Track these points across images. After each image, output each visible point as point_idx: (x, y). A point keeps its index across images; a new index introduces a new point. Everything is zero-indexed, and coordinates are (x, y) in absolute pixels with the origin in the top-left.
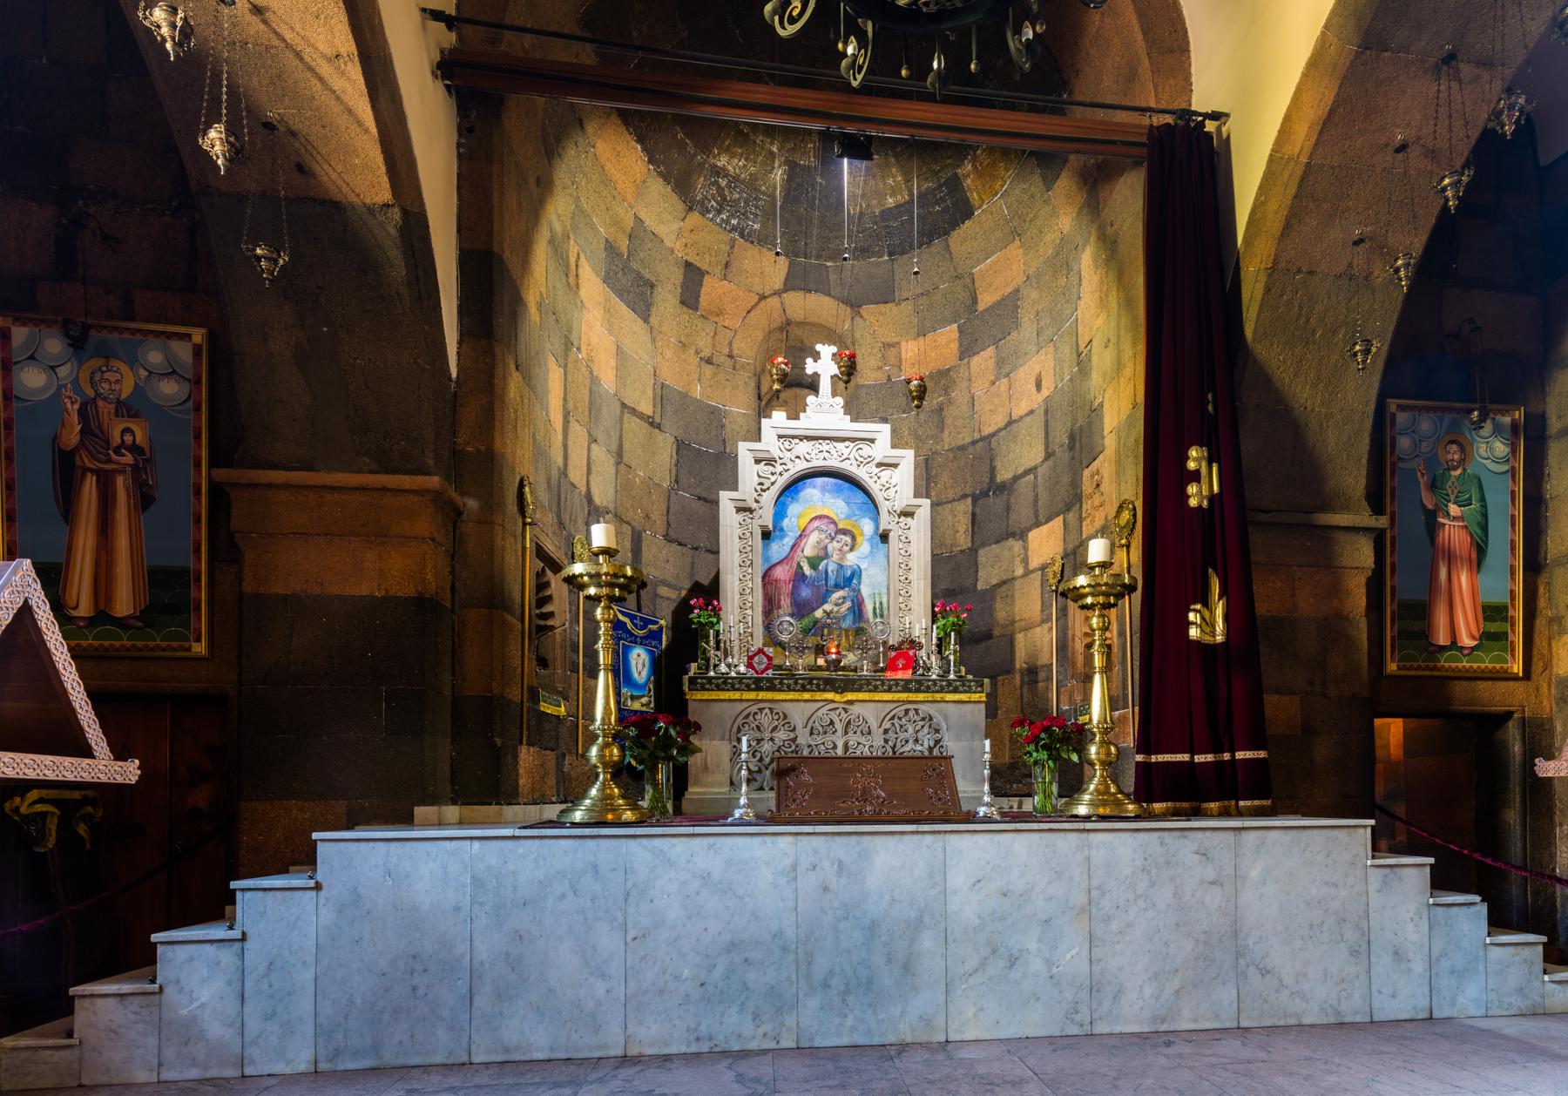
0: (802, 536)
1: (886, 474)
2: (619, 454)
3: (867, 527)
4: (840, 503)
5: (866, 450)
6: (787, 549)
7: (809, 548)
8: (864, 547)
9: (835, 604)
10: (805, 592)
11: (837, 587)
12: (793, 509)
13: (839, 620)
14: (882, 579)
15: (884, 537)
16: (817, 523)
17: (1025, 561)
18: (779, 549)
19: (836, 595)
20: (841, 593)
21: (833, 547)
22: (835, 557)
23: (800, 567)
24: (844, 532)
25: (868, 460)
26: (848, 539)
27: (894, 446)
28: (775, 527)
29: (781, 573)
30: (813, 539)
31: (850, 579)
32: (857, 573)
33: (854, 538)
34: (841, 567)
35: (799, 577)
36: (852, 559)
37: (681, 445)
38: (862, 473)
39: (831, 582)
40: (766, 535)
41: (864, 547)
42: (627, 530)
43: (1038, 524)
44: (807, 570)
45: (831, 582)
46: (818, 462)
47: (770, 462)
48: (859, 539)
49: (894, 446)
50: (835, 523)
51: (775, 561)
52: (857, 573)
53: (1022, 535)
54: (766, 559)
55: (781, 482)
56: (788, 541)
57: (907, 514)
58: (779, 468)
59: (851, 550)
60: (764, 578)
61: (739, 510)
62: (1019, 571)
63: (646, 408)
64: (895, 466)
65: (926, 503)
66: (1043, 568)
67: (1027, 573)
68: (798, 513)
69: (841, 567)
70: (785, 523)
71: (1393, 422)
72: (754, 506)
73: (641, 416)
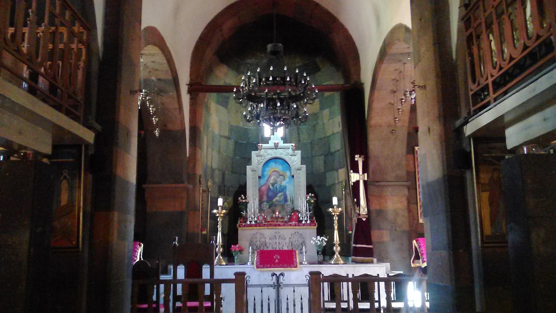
0: (270, 176)
1: (293, 157)
2: (219, 152)
3: (288, 173)
4: (280, 167)
5: (287, 151)
7: (271, 181)
8: (287, 180)
9: (278, 198)
10: (270, 194)
11: (280, 192)
12: (267, 169)
13: (280, 202)
15: (293, 176)
16: (274, 173)
17: (338, 178)
18: (263, 181)
19: (279, 194)
21: (278, 180)
22: (279, 183)
25: (288, 154)
28: (262, 174)
29: (264, 188)
30: (273, 178)
31: (283, 189)
32: (285, 188)
34: (280, 186)
35: (269, 189)
36: (284, 183)
37: (236, 143)
38: (286, 158)
39: (278, 191)
40: (260, 177)
41: (287, 180)
42: (221, 172)
43: (341, 168)
44: (271, 187)
45: (278, 191)
46: (274, 156)
47: (261, 156)
48: (286, 177)
51: (262, 184)
52: (285, 188)
53: (337, 170)
54: (259, 184)
55: (264, 162)
56: (266, 179)
58: (263, 158)
59: (284, 180)
61: (252, 171)
62: (337, 182)
63: (226, 134)
64: (295, 155)
65: (304, 166)
66: (342, 182)
67: (339, 183)
68: (269, 170)
70: (265, 173)
71: (417, 153)
72: (256, 169)
73: (225, 137)
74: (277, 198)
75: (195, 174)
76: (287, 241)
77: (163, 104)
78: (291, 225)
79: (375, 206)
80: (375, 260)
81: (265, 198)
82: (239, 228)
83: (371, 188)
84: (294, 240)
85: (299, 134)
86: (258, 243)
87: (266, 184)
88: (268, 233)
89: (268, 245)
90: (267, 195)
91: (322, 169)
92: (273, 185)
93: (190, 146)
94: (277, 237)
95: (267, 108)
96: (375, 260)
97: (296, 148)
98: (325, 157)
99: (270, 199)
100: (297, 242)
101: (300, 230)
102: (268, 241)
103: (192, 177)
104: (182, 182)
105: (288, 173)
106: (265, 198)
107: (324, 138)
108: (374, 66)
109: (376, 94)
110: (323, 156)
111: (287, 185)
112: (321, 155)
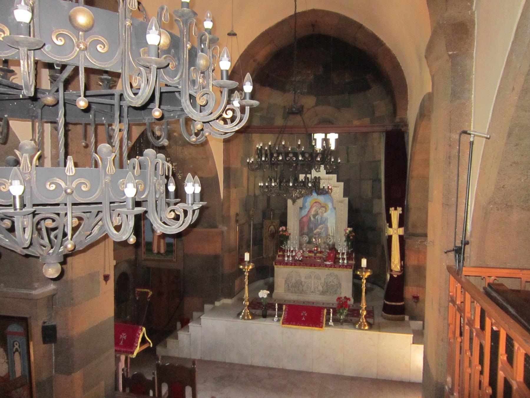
0: (311, 207)
3: (330, 205)
6: (307, 212)
7: (313, 212)
10: (311, 225)
11: (321, 224)
14: (334, 221)
16: (315, 204)
18: (304, 213)
19: (320, 227)
20: (322, 226)
22: (320, 214)
23: (310, 218)
24: (323, 207)
26: (324, 209)
27: (337, 181)
28: (303, 206)
29: (305, 219)
30: (314, 209)
31: (324, 222)
33: (326, 209)
34: (322, 217)
41: (329, 212)
44: (312, 218)
49: (337, 181)
50: (320, 204)
52: (327, 219)
56: (307, 210)
57: (341, 202)
59: (325, 212)
60: (300, 221)
69: (322, 217)
74: (318, 230)
75: (229, 217)
76: (323, 281)
77: (190, 154)
78: (326, 266)
79: (412, 261)
80: (407, 318)
81: (306, 230)
82: (275, 266)
83: (409, 242)
84: (330, 280)
85: (347, 154)
86: (293, 281)
87: (307, 215)
88: (304, 272)
89: (303, 284)
90: (308, 226)
91: (369, 194)
92: (314, 216)
93: (225, 187)
94: (313, 277)
95: (280, 185)
96: (407, 318)
97: (338, 180)
98: (373, 182)
99: (311, 230)
100: (332, 283)
101: (336, 271)
102: (303, 279)
103: (226, 219)
104: (216, 227)
105: (330, 205)
106: (306, 230)
107: (373, 161)
108: (415, 123)
109: (418, 146)
110: (371, 181)
111: (328, 217)
112: (370, 179)
